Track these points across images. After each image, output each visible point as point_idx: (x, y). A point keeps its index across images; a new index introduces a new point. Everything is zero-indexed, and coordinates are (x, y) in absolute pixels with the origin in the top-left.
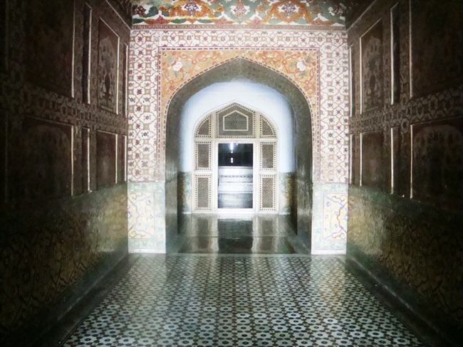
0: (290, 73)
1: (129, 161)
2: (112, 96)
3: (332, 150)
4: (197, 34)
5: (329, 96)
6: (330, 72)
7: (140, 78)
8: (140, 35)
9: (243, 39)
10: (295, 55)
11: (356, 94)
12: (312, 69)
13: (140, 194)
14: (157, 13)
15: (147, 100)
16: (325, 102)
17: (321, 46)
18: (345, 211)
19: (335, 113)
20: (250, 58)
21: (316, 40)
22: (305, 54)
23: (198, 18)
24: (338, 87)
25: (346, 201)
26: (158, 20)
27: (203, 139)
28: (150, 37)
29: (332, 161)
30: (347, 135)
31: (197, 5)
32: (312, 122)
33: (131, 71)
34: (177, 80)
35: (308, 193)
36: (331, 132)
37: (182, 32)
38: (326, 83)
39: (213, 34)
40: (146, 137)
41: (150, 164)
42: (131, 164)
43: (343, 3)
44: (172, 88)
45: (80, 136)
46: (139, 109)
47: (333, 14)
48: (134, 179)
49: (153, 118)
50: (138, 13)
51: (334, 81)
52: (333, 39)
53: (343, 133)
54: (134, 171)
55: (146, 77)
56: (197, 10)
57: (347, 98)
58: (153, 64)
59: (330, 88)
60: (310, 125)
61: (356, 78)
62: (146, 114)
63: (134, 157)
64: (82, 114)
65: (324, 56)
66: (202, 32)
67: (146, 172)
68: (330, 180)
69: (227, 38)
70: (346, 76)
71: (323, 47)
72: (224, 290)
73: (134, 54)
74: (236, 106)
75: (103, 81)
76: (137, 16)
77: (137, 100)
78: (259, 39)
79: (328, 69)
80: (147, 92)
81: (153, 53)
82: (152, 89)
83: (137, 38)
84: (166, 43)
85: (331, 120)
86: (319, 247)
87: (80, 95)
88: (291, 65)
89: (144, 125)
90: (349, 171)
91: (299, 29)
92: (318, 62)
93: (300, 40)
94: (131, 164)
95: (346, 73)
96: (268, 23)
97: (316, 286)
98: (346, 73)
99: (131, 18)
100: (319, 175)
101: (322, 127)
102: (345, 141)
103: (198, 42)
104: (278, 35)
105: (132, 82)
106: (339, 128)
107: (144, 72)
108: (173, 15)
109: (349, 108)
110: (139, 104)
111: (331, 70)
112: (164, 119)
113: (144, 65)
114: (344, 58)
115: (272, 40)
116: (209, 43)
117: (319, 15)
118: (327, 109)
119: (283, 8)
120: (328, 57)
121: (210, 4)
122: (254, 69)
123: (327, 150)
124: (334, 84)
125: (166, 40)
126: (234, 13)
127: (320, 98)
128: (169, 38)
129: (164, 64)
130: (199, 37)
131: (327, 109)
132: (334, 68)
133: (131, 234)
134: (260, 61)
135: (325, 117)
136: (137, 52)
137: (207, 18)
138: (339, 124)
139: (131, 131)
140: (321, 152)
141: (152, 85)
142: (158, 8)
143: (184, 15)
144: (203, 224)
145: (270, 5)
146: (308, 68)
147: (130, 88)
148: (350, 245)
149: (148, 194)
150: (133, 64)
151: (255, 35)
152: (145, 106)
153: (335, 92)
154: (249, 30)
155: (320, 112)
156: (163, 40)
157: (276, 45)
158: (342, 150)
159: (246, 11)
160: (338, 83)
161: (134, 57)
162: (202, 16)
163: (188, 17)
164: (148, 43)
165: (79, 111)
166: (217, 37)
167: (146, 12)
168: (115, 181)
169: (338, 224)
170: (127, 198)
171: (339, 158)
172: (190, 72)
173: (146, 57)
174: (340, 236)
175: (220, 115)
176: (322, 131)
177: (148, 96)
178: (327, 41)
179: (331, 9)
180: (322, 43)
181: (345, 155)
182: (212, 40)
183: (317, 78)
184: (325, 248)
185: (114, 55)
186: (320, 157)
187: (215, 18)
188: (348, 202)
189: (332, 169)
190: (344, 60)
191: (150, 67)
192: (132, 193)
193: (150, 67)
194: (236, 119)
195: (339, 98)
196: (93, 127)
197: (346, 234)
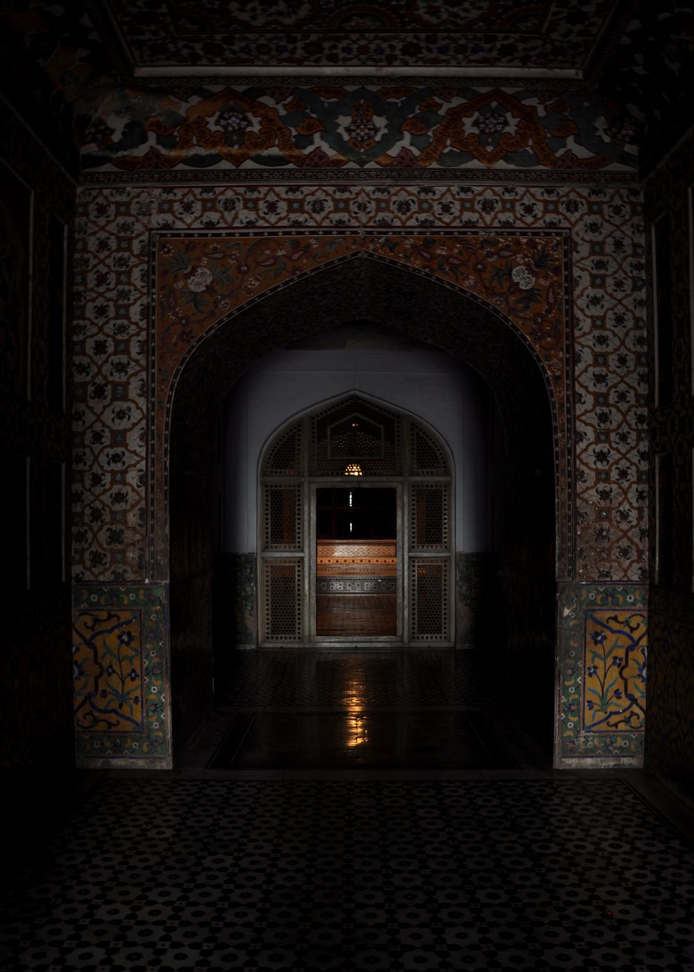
0: (495, 294)
1: (74, 530)
5: (596, 356)
6: (599, 293)
7: (101, 311)
8: (100, 200)
10: (507, 248)
12: (552, 285)
15: (121, 368)
16: (586, 371)
17: (574, 225)
18: (639, 656)
19: (613, 398)
21: (562, 209)
22: (532, 244)
23: (253, 153)
24: (620, 331)
25: (643, 628)
26: (147, 157)
28: (128, 205)
30: (643, 456)
31: (250, 115)
32: (554, 424)
33: (79, 294)
36: (603, 447)
37: (210, 189)
38: (589, 321)
39: (291, 196)
40: (118, 466)
41: (128, 536)
46: (99, 392)
47: (607, 139)
48: (88, 576)
49: (136, 415)
50: (94, 140)
51: (610, 315)
52: (605, 207)
53: (635, 452)
55: (118, 307)
56: (249, 129)
57: (643, 360)
58: (136, 273)
59: (597, 333)
62: (119, 405)
65: (584, 249)
67: (119, 556)
68: (601, 575)
69: (329, 205)
70: (640, 303)
73: (85, 250)
76: (92, 148)
77: (94, 369)
78: (414, 208)
79: (593, 285)
80: (122, 347)
81: (136, 246)
84: (169, 218)
86: (571, 750)
89: (114, 433)
92: (569, 266)
93: (519, 210)
94: (81, 537)
95: (643, 294)
96: (435, 165)
98: (643, 294)
100: (572, 561)
101: (580, 437)
103: (252, 216)
104: (463, 195)
105: (82, 323)
106: (623, 438)
107: (113, 295)
108: (186, 144)
109: (651, 386)
110: (99, 380)
111: (603, 286)
113: (112, 278)
114: (635, 255)
115: (446, 208)
116: (282, 217)
117: (570, 141)
118: (592, 389)
119: (476, 123)
120: (593, 253)
121: (283, 112)
123: (592, 496)
124: (610, 324)
125: (171, 211)
126: (346, 137)
127: (575, 359)
129: (164, 274)
130: (256, 201)
131: (592, 389)
132: (610, 281)
134: (417, 264)
136: (92, 244)
137: (274, 151)
138: (625, 429)
139: (80, 451)
140: (579, 502)
141: (133, 329)
143: (214, 145)
145: (442, 112)
146: (542, 282)
147: (75, 338)
149: (124, 616)
150: (84, 274)
151: (403, 196)
152: (115, 385)
153: (614, 343)
154: (388, 182)
155: (577, 398)
156: (161, 211)
158: (632, 495)
159: (377, 130)
160: (619, 320)
161: (86, 256)
163: (226, 150)
164: (121, 220)
166: (301, 202)
167: (116, 137)
169: (622, 689)
170: (70, 626)
171: (624, 516)
174: (627, 721)
176: (581, 446)
177: (124, 359)
178: (591, 212)
179: (600, 123)
180: (577, 215)
181: (640, 510)
182: (290, 210)
183: (564, 307)
184: (587, 753)
187: (297, 152)
188: (649, 632)
189: (606, 545)
190: (635, 261)
191: (130, 283)
192: (84, 613)
193: (130, 283)
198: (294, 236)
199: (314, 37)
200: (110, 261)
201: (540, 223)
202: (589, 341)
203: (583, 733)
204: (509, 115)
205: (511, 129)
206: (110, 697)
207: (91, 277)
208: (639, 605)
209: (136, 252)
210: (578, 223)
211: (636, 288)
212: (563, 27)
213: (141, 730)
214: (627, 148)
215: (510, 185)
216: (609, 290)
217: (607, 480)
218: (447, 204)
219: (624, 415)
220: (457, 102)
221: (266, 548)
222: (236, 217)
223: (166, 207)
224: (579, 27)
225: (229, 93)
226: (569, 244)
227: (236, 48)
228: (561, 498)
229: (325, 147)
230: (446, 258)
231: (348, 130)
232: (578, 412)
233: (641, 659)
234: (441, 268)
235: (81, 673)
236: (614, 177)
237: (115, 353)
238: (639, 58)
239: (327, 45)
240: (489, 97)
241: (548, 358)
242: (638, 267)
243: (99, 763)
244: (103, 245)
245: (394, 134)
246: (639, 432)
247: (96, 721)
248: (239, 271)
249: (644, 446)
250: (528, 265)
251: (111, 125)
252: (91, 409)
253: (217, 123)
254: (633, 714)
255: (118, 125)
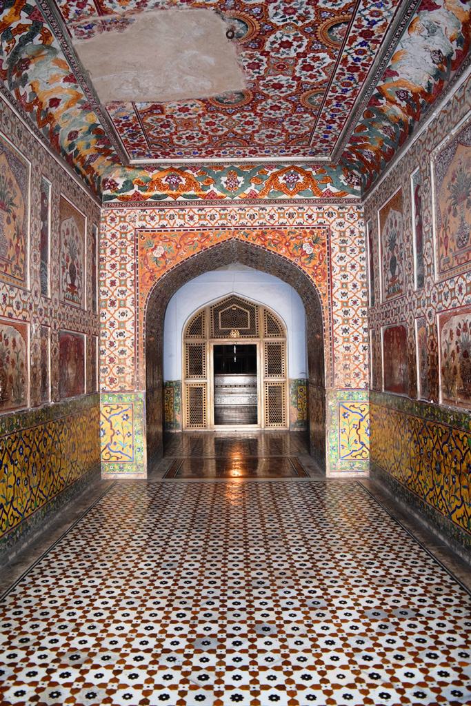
1: (102, 367)
2: (79, 288)
3: (347, 348)
4: (181, 212)
5: (342, 284)
6: (343, 255)
8: (112, 215)
9: (237, 217)
11: (375, 279)
13: (115, 407)
14: (133, 188)
15: (123, 292)
18: (365, 424)
19: (350, 303)
20: (246, 240)
21: (326, 216)
22: (312, 233)
23: (182, 193)
24: (353, 272)
25: (367, 410)
26: (134, 196)
27: (195, 341)
28: (125, 217)
29: (348, 362)
30: (365, 330)
34: (159, 269)
35: (320, 403)
36: (346, 326)
38: (339, 268)
40: (121, 338)
41: (127, 370)
42: (105, 370)
43: (356, 169)
44: (152, 278)
45: (39, 336)
46: (113, 303)
47: (346, 184)
48: (108, 389)
49: (130, 314)
50: (109, 188)
51: (349, 265)
52: (346, 214)
54: (107, 379)
55: (121, 265)
59: (342, 273)
60: (321, 319)
61: (374, 260)
62: (122, 310)
63: (107, 362)
64: (41, 310)
65: (336, 234)
66: (187, 210)
67: (122, 380)
69: (218, 217)
70: (363, 259)
71: (334, 224)
72: (214, 521)
73: (105, 238)
74: (233, 299)
75: (68, 270)
76: (108, 192)
77: (110, 294)
78: (257, 217)
79: (340, 251)
80: (123, 283)
81: (129, 236)
82: (129, 279)
83: (108, 218)
84: (144, 223)
85: (346, 313)
87: (38, 286)
88: (296, 247)
90: (370, 374)
91: (304, 202)
92: (329, 242)
93: (306, 217)
95: (364, 255)
96: (266, 197)
97: (329, 515)
98: (364, 255)
99: (101, 195)
101: (335, 322)
102: (364, 338)
105: (104, 272)
106: (356, 322)
107: (119, 259)
108: (152, 189)
109: (368, 298)
110: (113, 298)
111: (345, 251)
112: (143, 316)
113: (118, 251)
114: (360, 236)
115: (272, 217)
116: (196, 222)
117: (329, 185)
118: (340, 299)
119: (285, 179)
120: (340, 236)
121: (196, 176)
122: (252, 253)
123: (342, 349)
124: (349, 269)
125: (145, 220)
126: (225, 186)
127: (331, 286)
128: (148, 218)
129: (143, 248)
130: (184, 215)
131: (340, 299)
132: (348, 249)
133: (104, 456)
134: (258, 243)
135: (338, 309)
136: (109, 235)
137: (192, 193)
138: (356, 317)
141: (128, 275)
142: (133, 182)
143: (164, 190)
144: (197, 442)
146: (317, 250)
147: (101, 279)
148: (375, 465)
149: (125, 407)
150: (105, 249)
151: (252, 212)
152: (120, 301)
155: (333, 304)
156: (140, 220)
157: (277, 224)
158: (360, 348)
159: (239, 183)
160: (353, 267)
162: (186, 190)
163: (170, 192)
164: (122, 224)
165: (36, 306)
167: (120, 187)
168: (83, 391)
171: (357, 358)
172: (173, 258)
173: (121, 241)
174: (361, 455)
175: (216, 309)
176: (335, 326)
177: (124, 289)
178: (339, 217)
179: (342, 177)
180: (333, 219)
184: (343, 470)
185: (80, 241)
186: (334, 358)
187: (202, 193)
189: (348, 371)
190: (360, 239)
191: (126, 254)
192: (106, 406)
193: (126, 254)
194: (235, 313)
195: (355, 286)
196: (55, 326)
197: (368, 452)
198: (202, 231)
199: (210, 149)
200: (117, 243)
201: (315, 223)
202: (339, 277)
203: (339, 460)
204: (299, 175)
205: (301, 180)
206: (118, 445)
207: (108, 251)
208: (365, 400)
209: (129, 239)
210: (333, 223)
211: (361, 252)
212: (319, 144)
213: (132, 460)
214: (355, 187)
215: (301, 205)
216: (348, 253)
217: (348, 341)
218: (270, 215)
219: (356, 311)
220: (275, 170)
221: (187, 377)
222: (175, 222)
223: (142, 218)
224: (325, 144)
225: (172, 169)
226: (329, 233)
227: (176, 152)
228: (327, 350)
229: (215, 190)
230: (272, 240)
231: (226, 183)
232: (334, 310)
233: (367, 426)
234: (269, 244)
235: (104, 434)
236: (349, 201)
237: (120, 286)
238: (354, 155)
239: (215, 151)
240: (290, 168)
241: (320, 286)
242: (362, 242)
243: (112, 477)
244: (114, 236)
245: (248, 183)
246: (363, 319)
247: (111, 456)
248: (177, 247)
249: (366, 325)
250: (310, 243)
251: (118, 182)
252: (109, 311)
253: (166, 180)
254: (363, 451)
255: (120, 182)
